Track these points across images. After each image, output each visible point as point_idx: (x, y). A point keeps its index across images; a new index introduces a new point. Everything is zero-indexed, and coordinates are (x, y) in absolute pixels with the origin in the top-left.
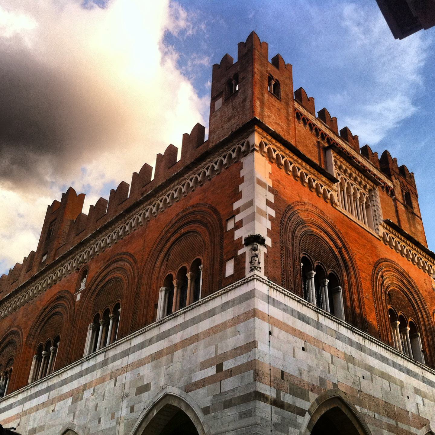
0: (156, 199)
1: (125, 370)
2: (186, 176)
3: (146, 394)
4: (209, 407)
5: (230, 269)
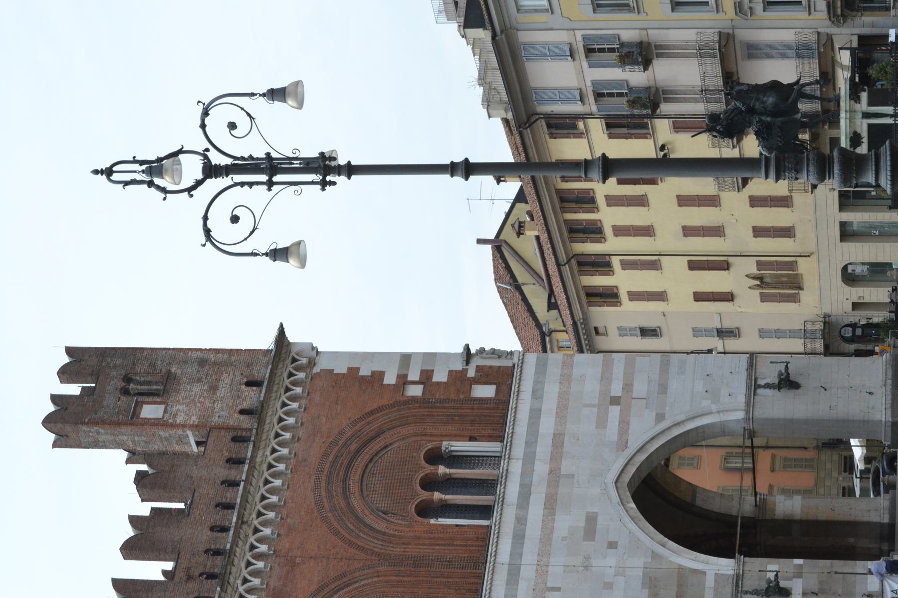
0: (244, 527)
1: (542, 569)
2: (258, 460)
3: (601, 522)
4: (657, 414)
5: (486, 391)
